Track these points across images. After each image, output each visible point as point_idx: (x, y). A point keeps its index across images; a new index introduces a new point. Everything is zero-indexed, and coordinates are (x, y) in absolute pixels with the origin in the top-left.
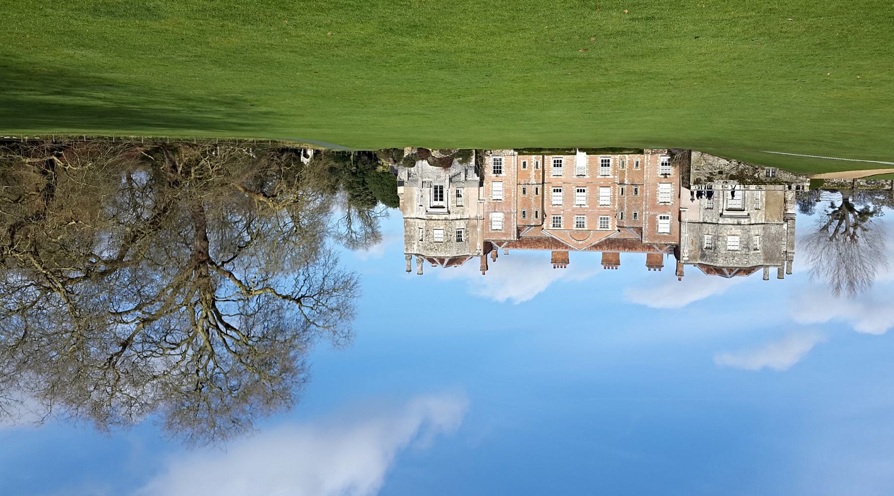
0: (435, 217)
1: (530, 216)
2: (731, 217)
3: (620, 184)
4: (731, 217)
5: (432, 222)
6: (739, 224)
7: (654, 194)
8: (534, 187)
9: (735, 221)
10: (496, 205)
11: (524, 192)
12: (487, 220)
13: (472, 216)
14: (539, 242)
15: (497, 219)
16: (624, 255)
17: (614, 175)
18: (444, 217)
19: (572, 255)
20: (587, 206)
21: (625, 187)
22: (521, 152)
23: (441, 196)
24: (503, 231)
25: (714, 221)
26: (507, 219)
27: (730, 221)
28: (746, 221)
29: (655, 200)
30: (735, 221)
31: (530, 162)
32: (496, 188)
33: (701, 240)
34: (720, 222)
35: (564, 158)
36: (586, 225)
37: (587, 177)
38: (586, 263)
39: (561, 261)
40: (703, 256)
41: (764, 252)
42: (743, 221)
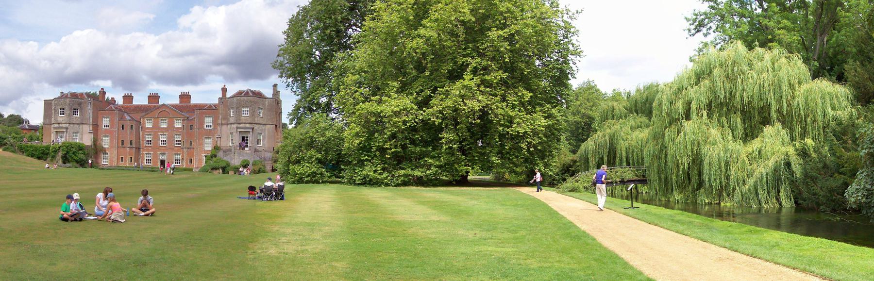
0: (248, 125)
2: (62, 128)
7: (111, 141)
10: (209, 134)
13: (224, 127)
18: (241, 125)
19: (177, 101)
21: (129, 145)
26: (202, 123)
27: (64, 125)
40: (80, 104)
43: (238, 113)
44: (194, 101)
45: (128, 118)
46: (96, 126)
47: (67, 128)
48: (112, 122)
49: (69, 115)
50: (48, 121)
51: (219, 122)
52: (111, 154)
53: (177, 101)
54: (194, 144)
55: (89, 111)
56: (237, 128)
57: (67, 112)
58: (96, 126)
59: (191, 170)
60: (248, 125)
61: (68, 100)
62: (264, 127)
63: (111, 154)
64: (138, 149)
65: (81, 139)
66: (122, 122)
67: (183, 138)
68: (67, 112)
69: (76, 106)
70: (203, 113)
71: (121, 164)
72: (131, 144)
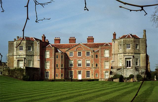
0: (130, 54)
1: (94, 55)
2: (21, 58)
4: (21, 58)
8: (93, 67)
9: (21, 56)
10: (107, 60)
12: (110, 54)
13: (116, 56)
14: (97, 46)
15: (107, 54)
16: (68, 43)
18: (126, 54)
20: (77, 60)
22: (98, 80)
23: (127, 63)
26: (102, 54)
27: (22, 56)
30: (21, 56)
31: (94, 76)
32: (107, 66)
35: (86, 78)
36: (77, 53)
37: (77, 71)
38: (82, 40)
39: (91, 39)
41: (14, 46)
42: (18, 57)
43: (125, 49)
44: (96, 41)
46: (71, 61)
49: (26, 50)
50: (11, 54)
54: (99, 65)
55: (37, 48)
58: (71, 61)
59: (98, 80)
62: (139, 55)
65: (33, 64)
66: (57, 53)
67: (92, 62)
68: (24, 48)
70: (104, 48)
71: (57, 78)
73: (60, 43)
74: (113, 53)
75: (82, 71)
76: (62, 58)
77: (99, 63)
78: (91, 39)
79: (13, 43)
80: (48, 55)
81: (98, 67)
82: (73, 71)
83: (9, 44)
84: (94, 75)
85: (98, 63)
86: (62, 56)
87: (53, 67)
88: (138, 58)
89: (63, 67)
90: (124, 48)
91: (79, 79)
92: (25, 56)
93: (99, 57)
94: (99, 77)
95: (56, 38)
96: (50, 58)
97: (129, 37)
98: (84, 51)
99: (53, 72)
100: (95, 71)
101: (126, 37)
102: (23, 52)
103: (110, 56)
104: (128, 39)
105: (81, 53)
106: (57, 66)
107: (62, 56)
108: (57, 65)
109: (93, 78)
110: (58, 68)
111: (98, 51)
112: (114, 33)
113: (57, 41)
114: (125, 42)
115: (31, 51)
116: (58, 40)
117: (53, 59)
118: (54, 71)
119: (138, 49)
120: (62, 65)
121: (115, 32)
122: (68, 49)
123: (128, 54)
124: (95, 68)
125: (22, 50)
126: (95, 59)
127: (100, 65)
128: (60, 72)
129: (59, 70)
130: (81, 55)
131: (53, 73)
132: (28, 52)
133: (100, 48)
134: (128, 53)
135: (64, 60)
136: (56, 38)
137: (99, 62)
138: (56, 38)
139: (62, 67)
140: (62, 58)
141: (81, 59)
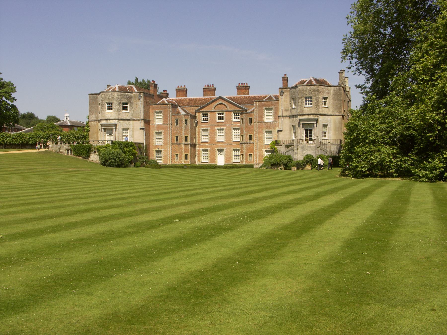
1: (246, 119)
3: (188, 144)
5: (313, 113)
6: (107, 120)
7: (165, 138)
11: (250, 136)
17: (199, 150)
20: (216, 128)
21: (184, 142)
22: (252, 166)
24: (264, 108)
25: (121, 121)
26: (261, 117)
28: (104, 122)
29: (164, 133)
30: (109, 122)
31: (246, 159)
33: (131, 109)
34: (117, 121)
37: (216, 149)
40: (130, 98)
44: (253, 93)
45: (182, 112)
47: (116, 125)
48: (165, 119)
49: (118, 110)
50: (93, 117)
51: (280, 114)
52: (166, 151)
53: (234, 93)
56: (300, 120)
57: (115, 106)
60: (311, 117)
61: (115, 94)
63: (166, 151)
64: (193, 146)
68: (115, 106)
69: (125, 101)
71: (177, 162)
72: (186, 140)
73: (186, 96)
74: (280, 114)
75: (225, 149)
76: (186, 123)
77: (254, 135)
78: (243, 88)
79: (97, 98)
80: (158, 120)
81: (252, 141)
82: (209, 149)
83: (90, 98)
84: (246, 156)
85: (252, 134)
86: (186, 121)
87: (169, 140)
88: (326, 124)
89: (189, 142)
90: (300, 104)
91: (218, 165)
92: (116, 122)
93: (255, 123)
94: (254, 161)
95: (178, 86)
96: (164, 123)
97: (310, 83)
98: (230, 110)
99: (169, 151)
100: (247, 150)
101: (305, 84)
102: (112, 113)
103: (275, 121)
104: (308, 88)
105: (224, 114)
106: (177, 140)
107: (186, 121)
108: (177, 137)
109: (244, 163)
110: (180, 144)
111: (254, 111)
112: (283, 76)
113: (181, 93)
114: (302, 93)
115: (128, 111)
116: (182, 91)
117: (169, 126)
118: (171, 149)
119: (327, 106)
120: (186, 137)
121: (285, 75)
122: (199, 108)
123: (307, 116)
124: (248, 143)
125: (112, 109)
126: (247, 126)
127: (256, 137)
128: (183, 151)
129: (181, 146)
130: (224, 118)
131: (169, 153)
132: (121, 113)
133: (256, 104)
134: (308, 115)
135: (189, 129)
136: (180, 87)
137: (255, 132)
138: (180, 87)
139: (186, 140)
140: (186, 123)
141: (223, 126)
